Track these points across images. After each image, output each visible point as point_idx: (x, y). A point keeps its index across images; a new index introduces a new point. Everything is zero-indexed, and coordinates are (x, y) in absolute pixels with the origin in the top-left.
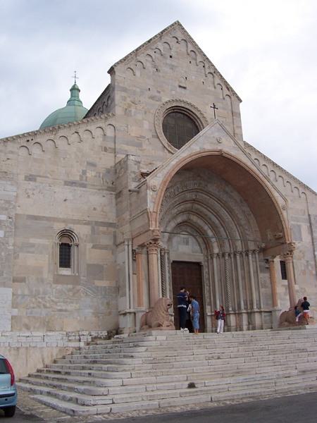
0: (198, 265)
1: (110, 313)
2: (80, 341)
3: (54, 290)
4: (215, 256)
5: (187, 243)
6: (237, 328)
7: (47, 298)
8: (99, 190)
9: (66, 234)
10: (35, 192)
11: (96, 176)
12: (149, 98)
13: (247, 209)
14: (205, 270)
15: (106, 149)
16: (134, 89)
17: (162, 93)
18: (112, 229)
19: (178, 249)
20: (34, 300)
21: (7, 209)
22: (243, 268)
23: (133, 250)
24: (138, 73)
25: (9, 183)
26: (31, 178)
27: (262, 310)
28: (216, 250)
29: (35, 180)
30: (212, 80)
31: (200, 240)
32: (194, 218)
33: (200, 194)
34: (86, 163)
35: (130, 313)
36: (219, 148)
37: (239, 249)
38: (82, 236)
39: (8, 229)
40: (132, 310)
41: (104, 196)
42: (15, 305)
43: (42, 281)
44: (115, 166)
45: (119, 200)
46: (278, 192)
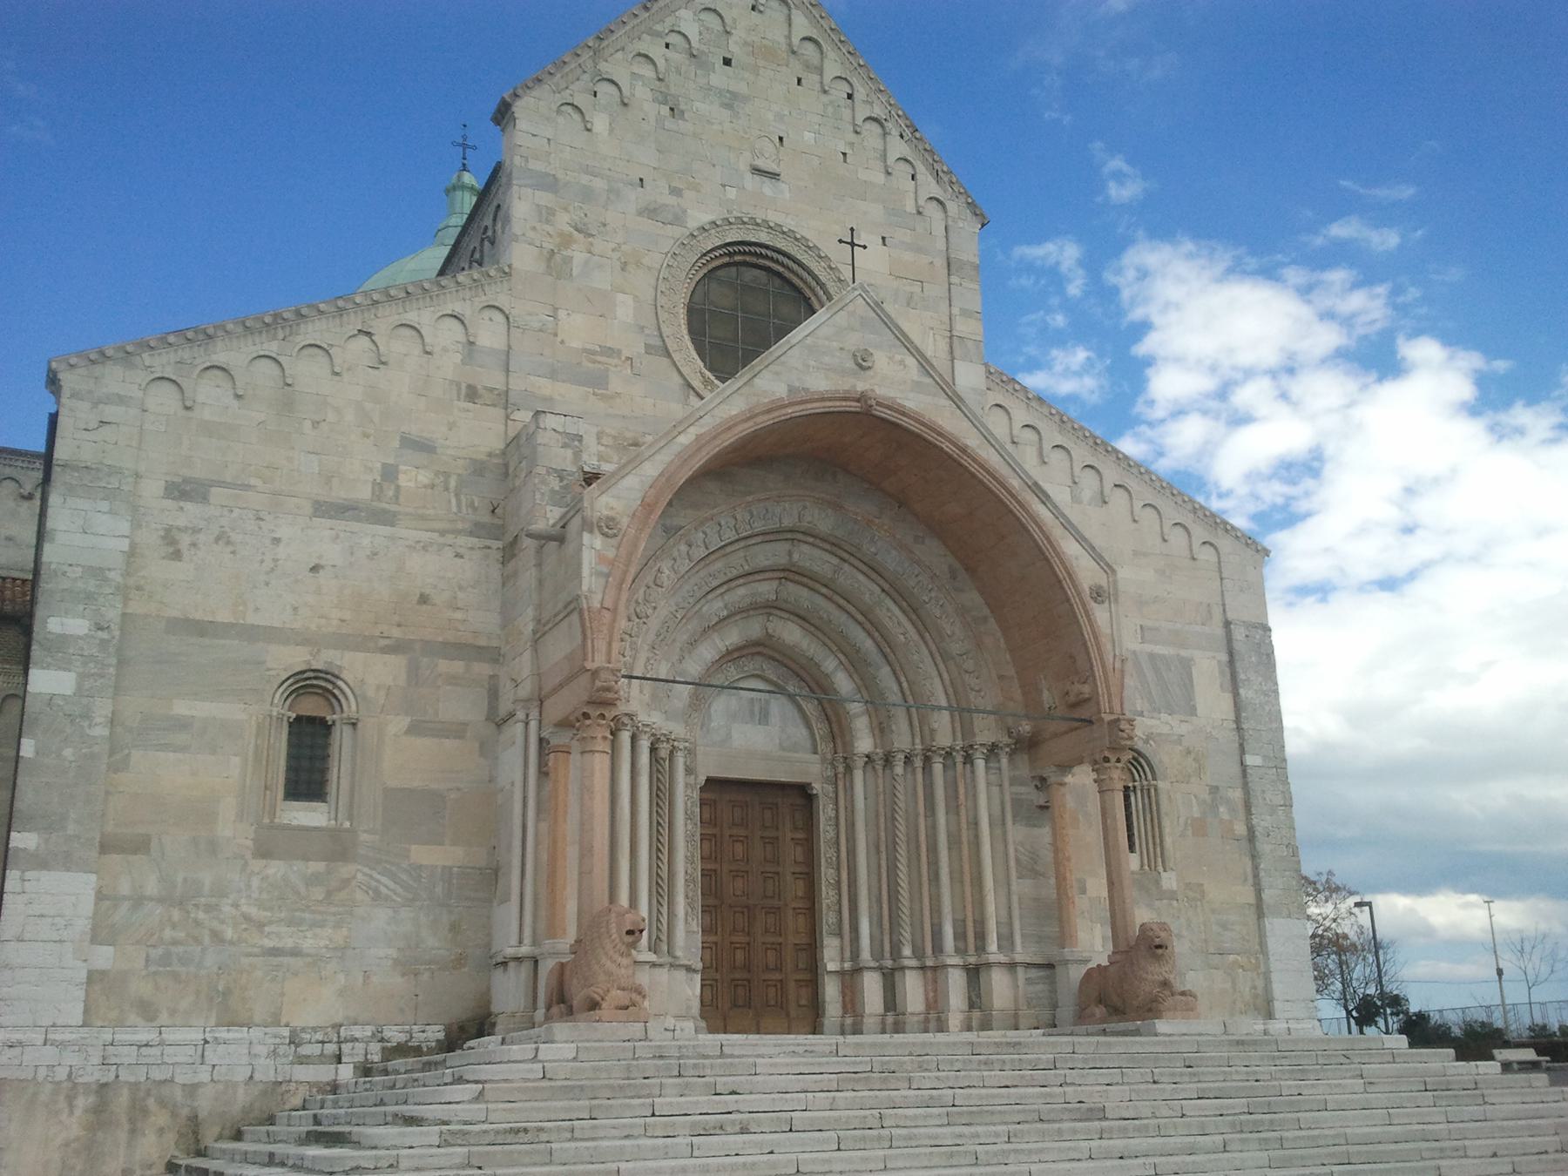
0: (803, 793)
1: (460, 961)
2: (339, 1059)
3: (255, 882)
4: (860, 762)
5: (764, 718)
6: (927, 1020)
7: (227, 909)
8: (443, 533)
9: (314, 684)
10: (201, 537)
11: (433, 486)
12: (640, 214)
13: (973, 598)
14: (825, 811)
15: (472, 394)
16: (585, 179)
17: (687, 193)
18: (483, 669)
20: (176, 914)
21: (90, 597)
22: (953, 807)
23: (541, 740)
24: (600, 123)
25: (105, 506)
26: (182, 491)
27: (1019, 958)
28: (864, 743)
29: (204, 499)
30: (879, 144)
31: (810, 708)
32: (791, 634)
33: (805, 548)
34: (396, 444)
35: (518, 959)
36: (861, 387)
37: (944, 739)
38: (371, 693)
39: (92, 668)
40: (525, 950)
41: (458, 555)
42: (100, 933)
43: (213, 847)
44: (504, 453)
45: (511, 566)
46: (1081, 539)
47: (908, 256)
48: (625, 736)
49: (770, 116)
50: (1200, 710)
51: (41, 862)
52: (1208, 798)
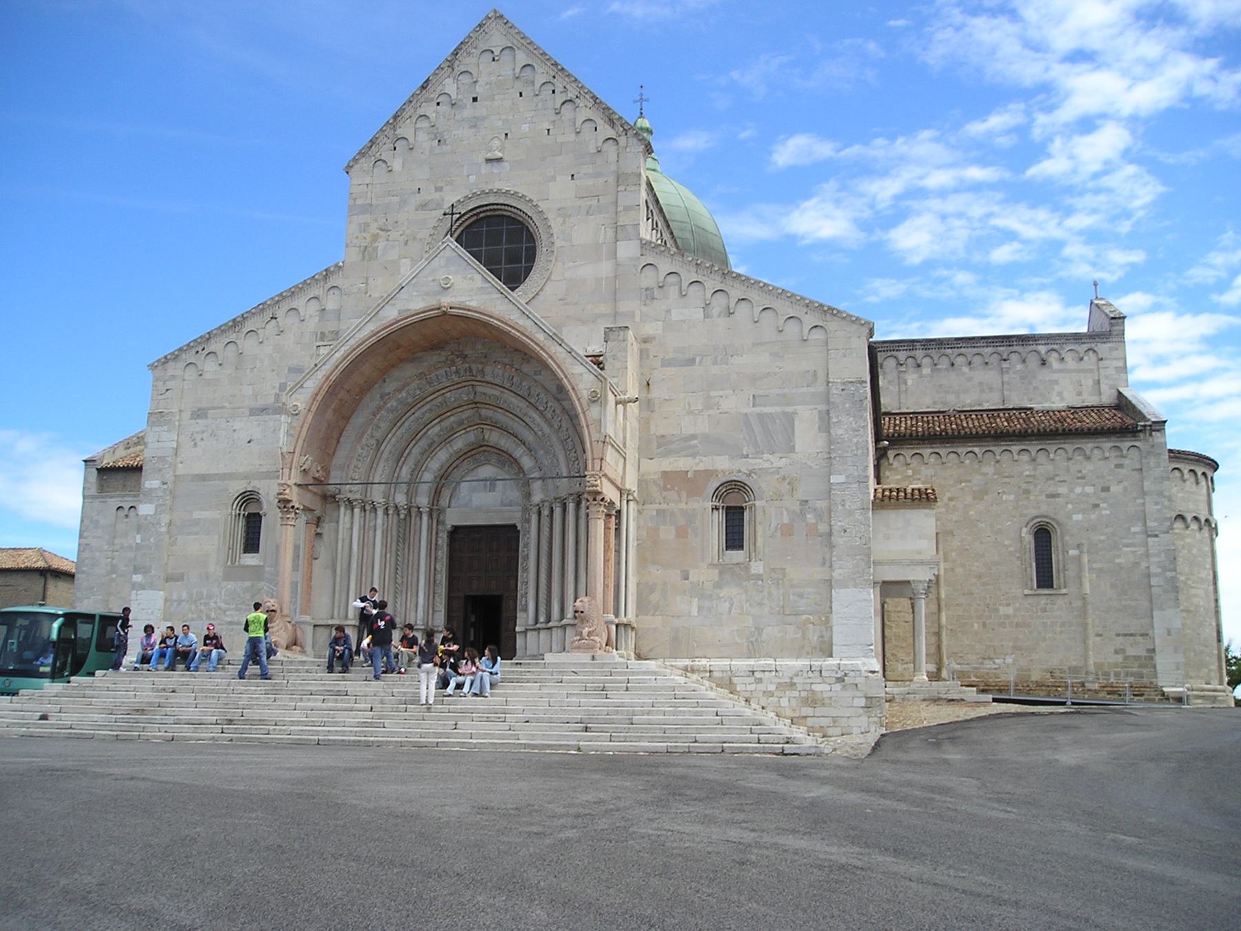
0: (513, 527)
9: (249, 498)
19: (471, 500)
20: (193, 607)
21: (160, 470)
24: (397, 165)
26: (199, 414)
32: (494, 437)
47: (590, 182)
48: (357, 511)
49: (500, 123)
50: (797, 448)
51: (142, 587)
52: (797, 508)
